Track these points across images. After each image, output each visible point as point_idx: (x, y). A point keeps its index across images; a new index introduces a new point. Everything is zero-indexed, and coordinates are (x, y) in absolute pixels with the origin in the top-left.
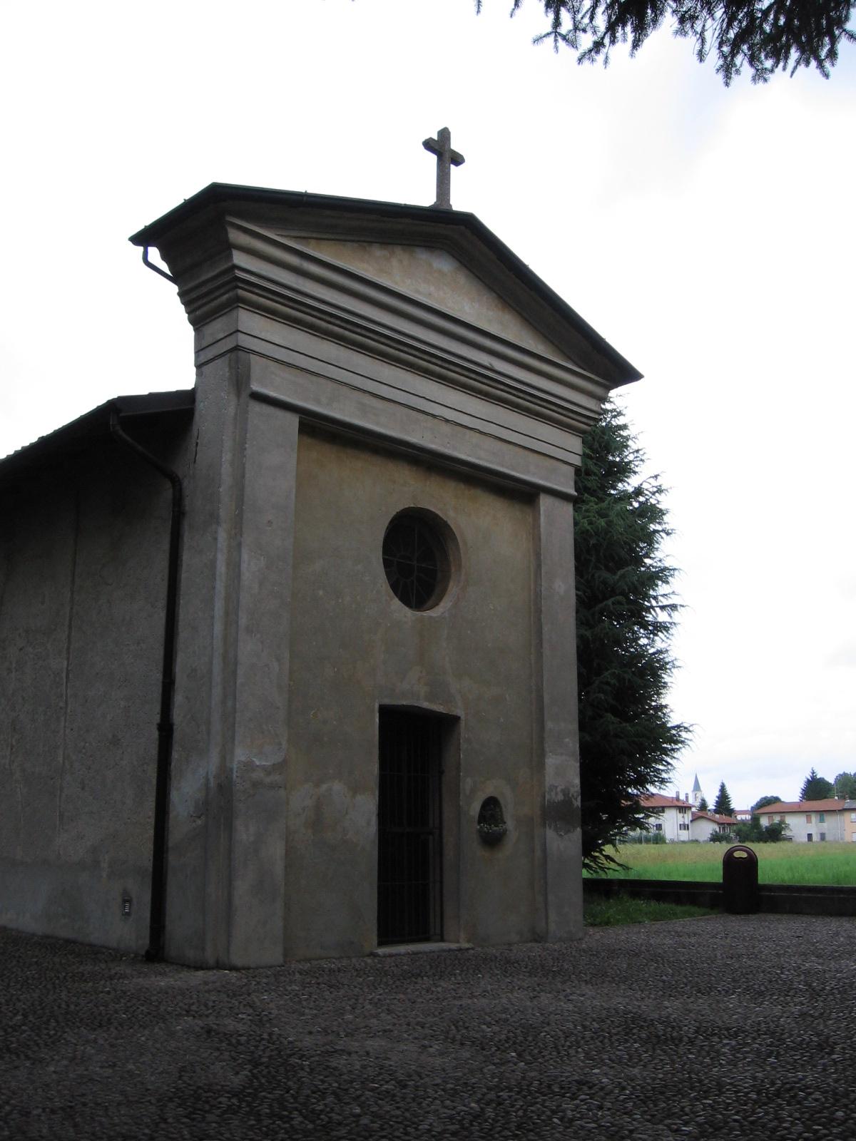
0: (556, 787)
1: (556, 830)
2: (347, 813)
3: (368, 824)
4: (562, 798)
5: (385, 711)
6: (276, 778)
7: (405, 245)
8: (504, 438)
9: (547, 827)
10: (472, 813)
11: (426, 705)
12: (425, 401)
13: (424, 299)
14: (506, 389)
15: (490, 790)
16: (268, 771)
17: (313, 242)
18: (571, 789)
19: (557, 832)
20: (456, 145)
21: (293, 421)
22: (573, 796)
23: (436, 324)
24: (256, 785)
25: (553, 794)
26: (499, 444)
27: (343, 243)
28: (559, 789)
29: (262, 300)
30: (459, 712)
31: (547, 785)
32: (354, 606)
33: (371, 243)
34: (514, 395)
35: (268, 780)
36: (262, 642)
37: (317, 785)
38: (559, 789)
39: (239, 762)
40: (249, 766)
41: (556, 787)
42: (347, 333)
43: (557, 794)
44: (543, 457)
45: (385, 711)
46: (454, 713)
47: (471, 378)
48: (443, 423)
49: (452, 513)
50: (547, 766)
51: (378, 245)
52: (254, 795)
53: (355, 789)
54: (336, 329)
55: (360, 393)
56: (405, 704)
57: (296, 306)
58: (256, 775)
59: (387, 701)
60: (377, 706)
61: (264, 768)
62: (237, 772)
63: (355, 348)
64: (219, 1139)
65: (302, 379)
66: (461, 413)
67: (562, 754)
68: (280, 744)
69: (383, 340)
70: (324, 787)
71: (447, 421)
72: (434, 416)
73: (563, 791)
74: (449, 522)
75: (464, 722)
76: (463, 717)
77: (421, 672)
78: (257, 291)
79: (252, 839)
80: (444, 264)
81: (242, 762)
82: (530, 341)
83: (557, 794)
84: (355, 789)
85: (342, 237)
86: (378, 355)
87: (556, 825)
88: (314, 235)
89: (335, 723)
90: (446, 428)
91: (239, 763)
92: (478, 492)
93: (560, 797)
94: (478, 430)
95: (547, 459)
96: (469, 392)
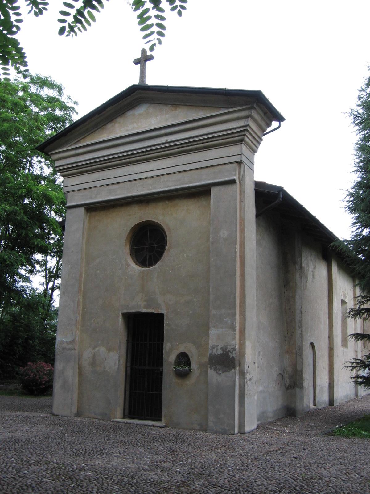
0: (217, 346)
1: (216, 370)
2: (106, 360)
3: (115, 364)
4: (222, 352)
5: (124, 315)
6: (70, 346)
7: (121, 115)
8: (223, 163)
9: (209, 369)
10: (170, 360)
11: (144, 310)
12: (139, 174)
13: (90, 142)
14: (179, 146)
15: (182, 349)
16: (68, 344)
17: (82, 140)
18: (229, 346)
19: (216, 372)
20: (139, 56)
21: (82, 210)
22: (229, 351)
23: (116, 144)
24: (63, 349)
25: (214, 350)
26: (182, 174)
27: (94, 133)
28: (219, 348)
29: (68, 172)
30: (163, 311)
31: (210, 345)
32: (111, 274)
33: (106, 124)
34: (186, 147)
35: (68, 347)
36: (68, 296)
37: (94, 348)
38: (219, 348)
39: (59, 341)
40: (62, 342)
41: (217, 346)
42: (99, 166)
43: (217, 350)
44: (212, 168)
45: (124, 315)
46: (160, 313)
47: (137, 157)
48: (149, 179)
49: (161, 218)
50: (210, 336)
51: (109, 123)
52: (63, 353)
53: (109, 350)
54: (94, 167)
55: (109, 186)
56: (133, 311)
57: (78, 168)
58: (64, 345)
59: (125, 311)
60: (120, 314)
61: (66, 342)
62: (58, 344)
63: (151, 160)
64: (137, 493)
65: (86, 192)
66: (158, 170)
67: (222, 328)
68: (73, 333)
69: (113, 160)
70: (97, 349)
71: (151, 177)
72: (143, 179)
73: (221, 348)
74: (159, 222)
75: (166, 316)
76: (165, 314)
77: (142, 296)
78: (65, 171)
79: (61, 369)
80: (141, 110)
81: (60, 341)
82: (193, 115)
83: (217, 350)
84: (109, 350)
85: (92, 131)
86: (115, 167)
87: (216, 368)
88: (81, 138)
89: (102, 323)
90: (150, 181)
91: (58, 341)
92: (177, 201)
93: (220, 352)
94: (168, 173)
95: (216, 167)
96: (126, 165)
